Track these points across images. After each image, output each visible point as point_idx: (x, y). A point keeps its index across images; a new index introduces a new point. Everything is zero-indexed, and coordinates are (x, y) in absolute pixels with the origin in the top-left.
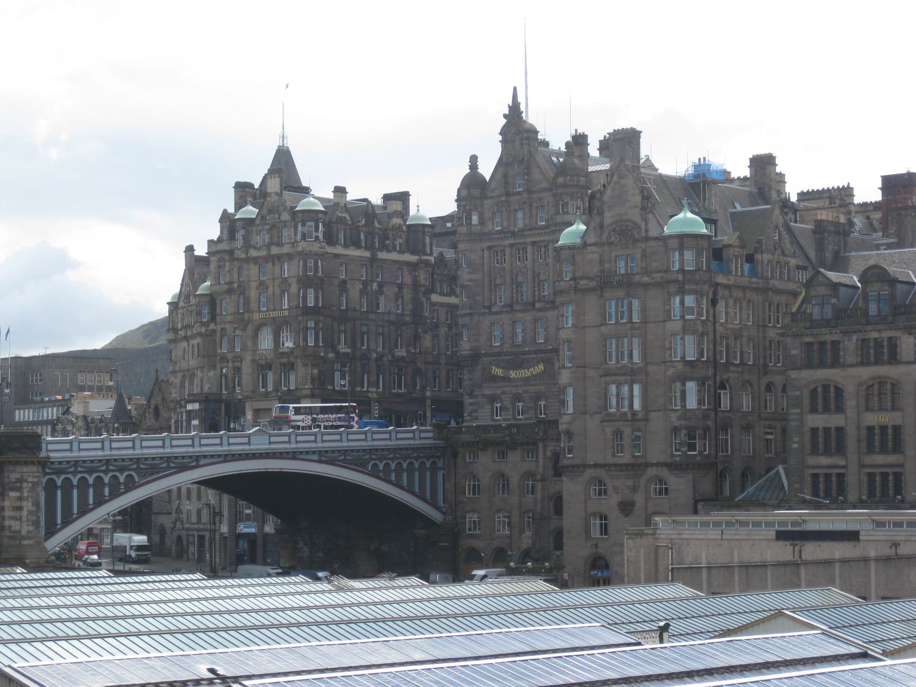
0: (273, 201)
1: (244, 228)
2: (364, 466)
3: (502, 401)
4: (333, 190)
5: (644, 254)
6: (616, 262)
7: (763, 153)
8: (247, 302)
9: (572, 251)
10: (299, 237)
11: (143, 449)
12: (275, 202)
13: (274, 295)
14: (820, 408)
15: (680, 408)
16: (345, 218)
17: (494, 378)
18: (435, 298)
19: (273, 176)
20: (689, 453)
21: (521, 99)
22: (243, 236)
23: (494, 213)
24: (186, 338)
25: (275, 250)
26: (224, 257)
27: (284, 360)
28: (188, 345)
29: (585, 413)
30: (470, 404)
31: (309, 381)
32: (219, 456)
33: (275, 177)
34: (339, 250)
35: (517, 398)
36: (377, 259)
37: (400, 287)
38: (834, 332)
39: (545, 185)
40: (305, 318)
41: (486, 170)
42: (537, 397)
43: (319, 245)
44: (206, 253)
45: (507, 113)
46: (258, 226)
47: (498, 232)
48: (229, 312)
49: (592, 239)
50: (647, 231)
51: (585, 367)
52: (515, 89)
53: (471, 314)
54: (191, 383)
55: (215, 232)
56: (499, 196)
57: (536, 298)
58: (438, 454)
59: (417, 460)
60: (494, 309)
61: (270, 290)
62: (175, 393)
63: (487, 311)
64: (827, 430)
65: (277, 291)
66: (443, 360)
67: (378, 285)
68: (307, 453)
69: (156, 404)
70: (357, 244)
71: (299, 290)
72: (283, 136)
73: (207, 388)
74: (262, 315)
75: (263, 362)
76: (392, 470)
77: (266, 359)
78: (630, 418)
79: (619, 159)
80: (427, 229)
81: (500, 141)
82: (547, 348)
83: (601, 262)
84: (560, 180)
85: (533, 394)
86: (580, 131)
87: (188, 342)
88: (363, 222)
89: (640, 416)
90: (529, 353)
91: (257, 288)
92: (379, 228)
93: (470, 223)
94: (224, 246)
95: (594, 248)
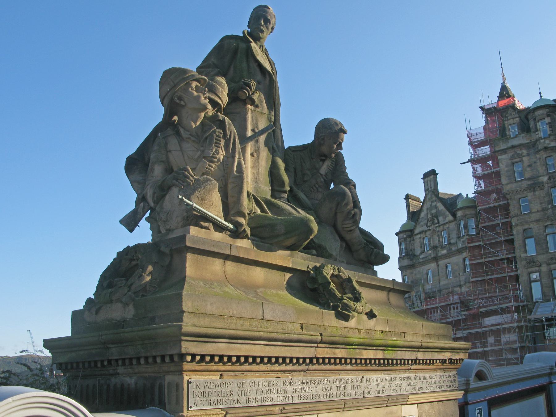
1: (548, 116)
24: (436, 259)
28: (438, 266)
48: (533, 211)
87: (437, 262)
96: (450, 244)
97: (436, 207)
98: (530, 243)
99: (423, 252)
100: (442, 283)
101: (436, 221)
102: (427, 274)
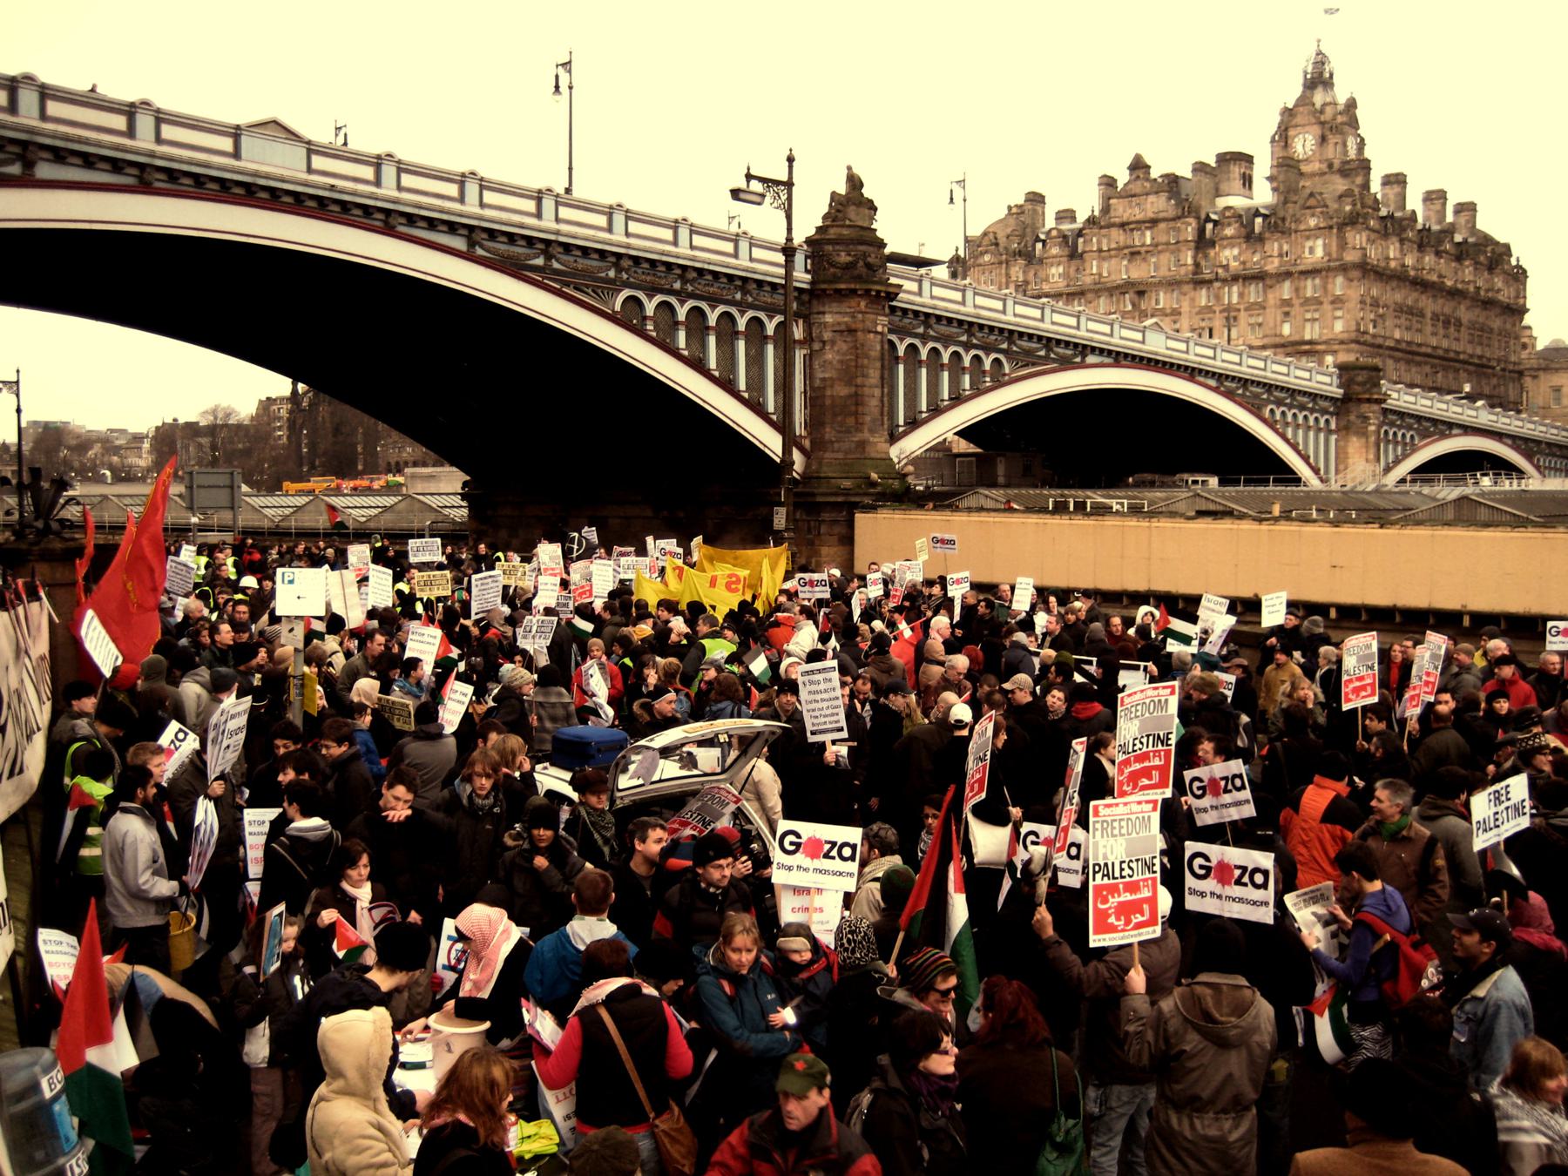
32: (1110, 352)
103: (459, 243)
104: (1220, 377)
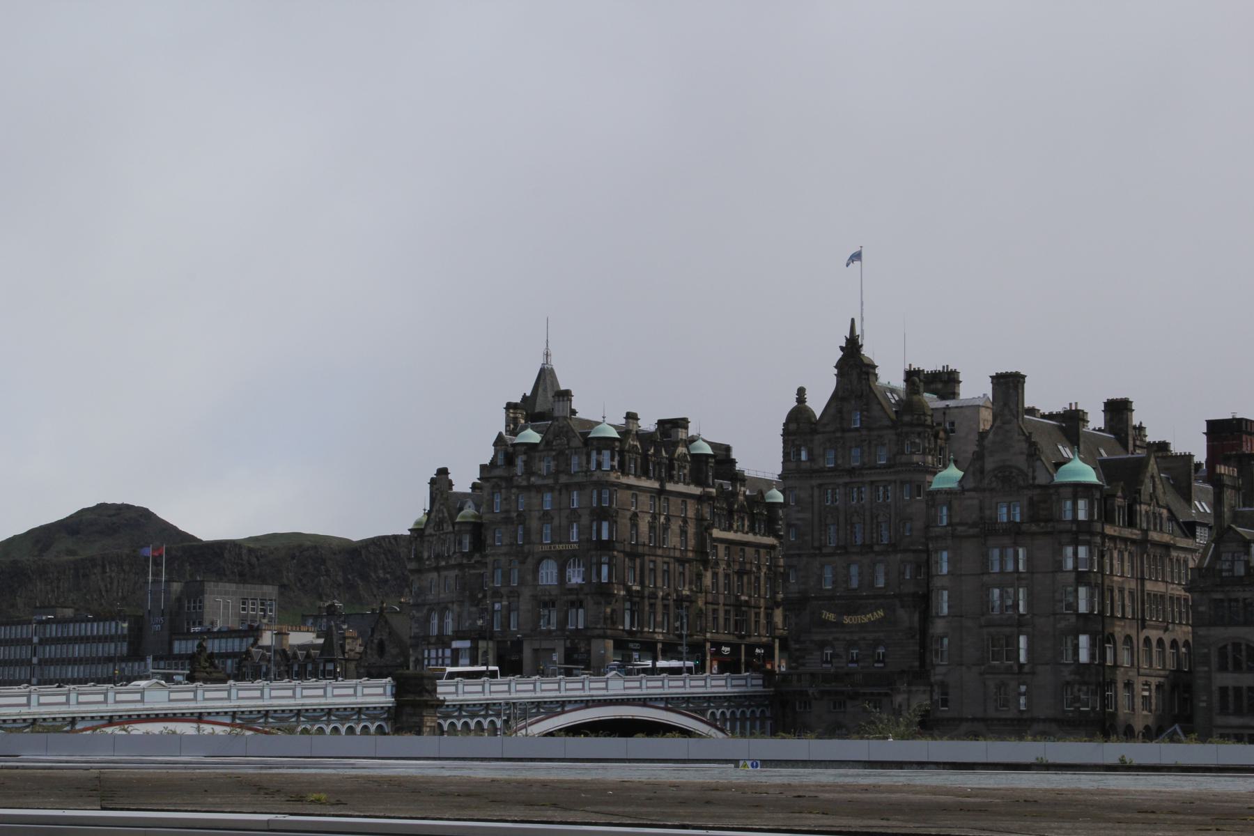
0: (561, 425)
1: (525, 453)
2: (703, 713)
3: (833, 647)
4: (625, 416)
5: (1032, 503)
6: (997, 508)
7: (1119, 397)
8: (527, 533)
9: (949, 497)
10: (593, 466)
11: (492, 694)
12: (563, 427)
13: (560, 526)
14: (1230, 666)
15: (1072, 662)
16: (636, 446)
17: (825, 623)
18: (716, 533)
19: (561, 399)
20: (1082, 709)
21: (858, 332)
22: (524, 461)
23: (825, 449)
24: (437, 569)
25: (563, 479)
26: (499, 483)
27: (573, 597)
28: (439, 576)
29: (961, 665)
30: (797, 650)
31: (602, 621)
32: (582, 701)
33: (559, 401)
34: (631, 480)
35: (851, 644)
36: (666, 490)
37: (685, 521)
38: (1246, 589)
39: (887, 423)
40: (599, 552)
41: (817, 404)
42: (877, 643)
43: (615, 475)
44: (478, 479)
45: (844, 346)
46: (542, 451)
47: (831, 470)
48: (504, 543)
49: (970, 484)
50: (1034, 478)
51: (961, 616)
52: (853, 320)
53: (799, 555)
54: (441, 619)
55: (487, 455)
56: (834, 432)
57: (875, 540)
58: (767, 703)
59: (748, 709)
60: (825, 551)
61: (556, 522)
62: (417, 628)
63: (817, 552)
64: (1238, 690)
65: (564, 522)
66: (721, 600)
67: (665, 519)
68: (656, 699)
69: (381, 639)
70: (645, 473)
71: (592, 521)
72: (547, 355)
73: (467, 624)
74: (546, 548)
75: (547, 598)
76: (737, 719)
77: (550, 595)
78: (1017, 671)
79: (1001, 404)
80: (710, 460)
81: (835, 375)
82: (887, 593)
83: (981, 509)
84: (907, 418)
85: (871, 642)
86: (915, 366)
87: (439, 572)
88: (652, 451)
89: (1026, 669)
90: (867, 597)
91: (540, 519)
92: (666, 458)
93: (800, 459)
94: (497, 472)
95: (973, 494)
96: (449, 556)
97: (443, 513)
98: (499, 573)
99: (429, 558)
100: (442, 596)
101: (441, 528)
102: (431, 582)
103: (228, 720)
104: (667, 700)
